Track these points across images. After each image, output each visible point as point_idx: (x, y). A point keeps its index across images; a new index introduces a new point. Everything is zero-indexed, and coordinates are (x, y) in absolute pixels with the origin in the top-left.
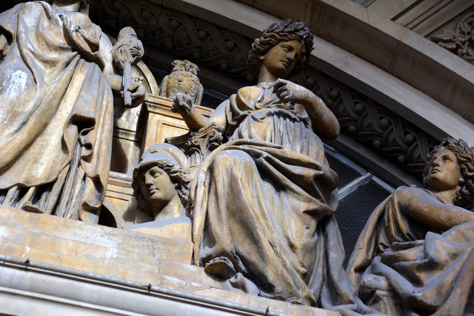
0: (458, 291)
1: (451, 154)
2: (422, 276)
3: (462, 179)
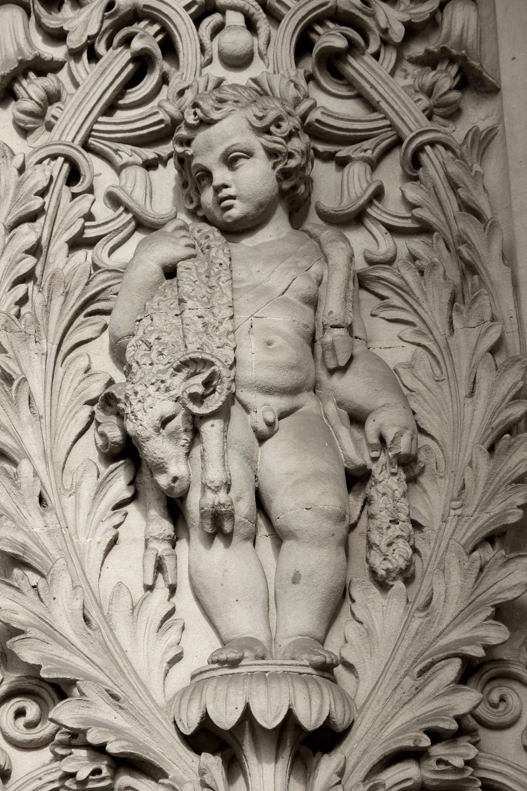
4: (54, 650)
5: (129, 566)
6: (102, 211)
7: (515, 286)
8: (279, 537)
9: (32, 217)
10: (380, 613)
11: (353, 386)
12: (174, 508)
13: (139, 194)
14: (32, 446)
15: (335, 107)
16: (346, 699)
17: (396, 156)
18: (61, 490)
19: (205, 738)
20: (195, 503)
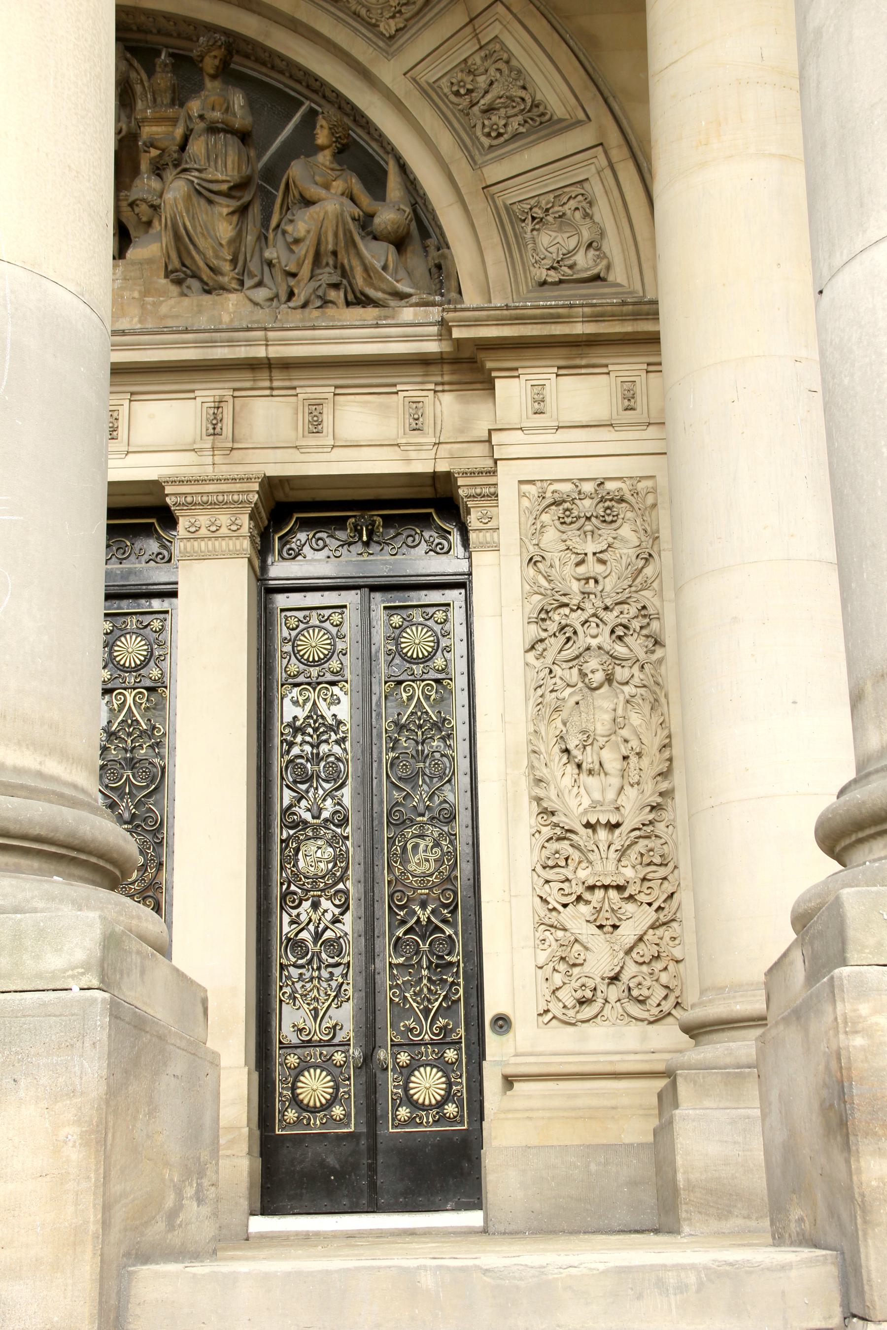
0: (306, 262)
1: (324, 123)
2: (294, 247)
3: (334, 139)
4: (551, 803)
5: (567, 781)
6: (559, 682)
7: (668, 703)
8: (606, 774)
9: (540, 686)
10: (631, 793)
11: (625, 733)
12: (579, 766)
13: (568, 677)
14: (543, 750)
15: (620, 650)
16: (622, 815)
17: (638, 663)
18: (550, 761)
19: (588, 825)
20: (584, 766)
